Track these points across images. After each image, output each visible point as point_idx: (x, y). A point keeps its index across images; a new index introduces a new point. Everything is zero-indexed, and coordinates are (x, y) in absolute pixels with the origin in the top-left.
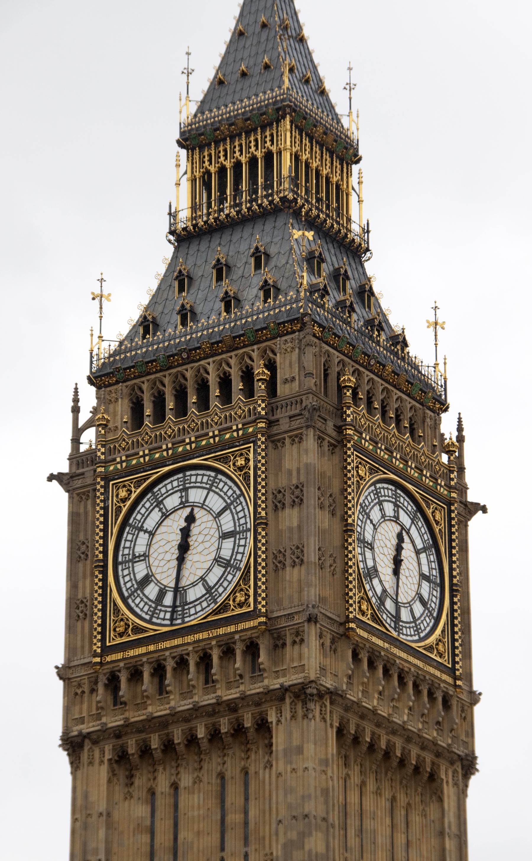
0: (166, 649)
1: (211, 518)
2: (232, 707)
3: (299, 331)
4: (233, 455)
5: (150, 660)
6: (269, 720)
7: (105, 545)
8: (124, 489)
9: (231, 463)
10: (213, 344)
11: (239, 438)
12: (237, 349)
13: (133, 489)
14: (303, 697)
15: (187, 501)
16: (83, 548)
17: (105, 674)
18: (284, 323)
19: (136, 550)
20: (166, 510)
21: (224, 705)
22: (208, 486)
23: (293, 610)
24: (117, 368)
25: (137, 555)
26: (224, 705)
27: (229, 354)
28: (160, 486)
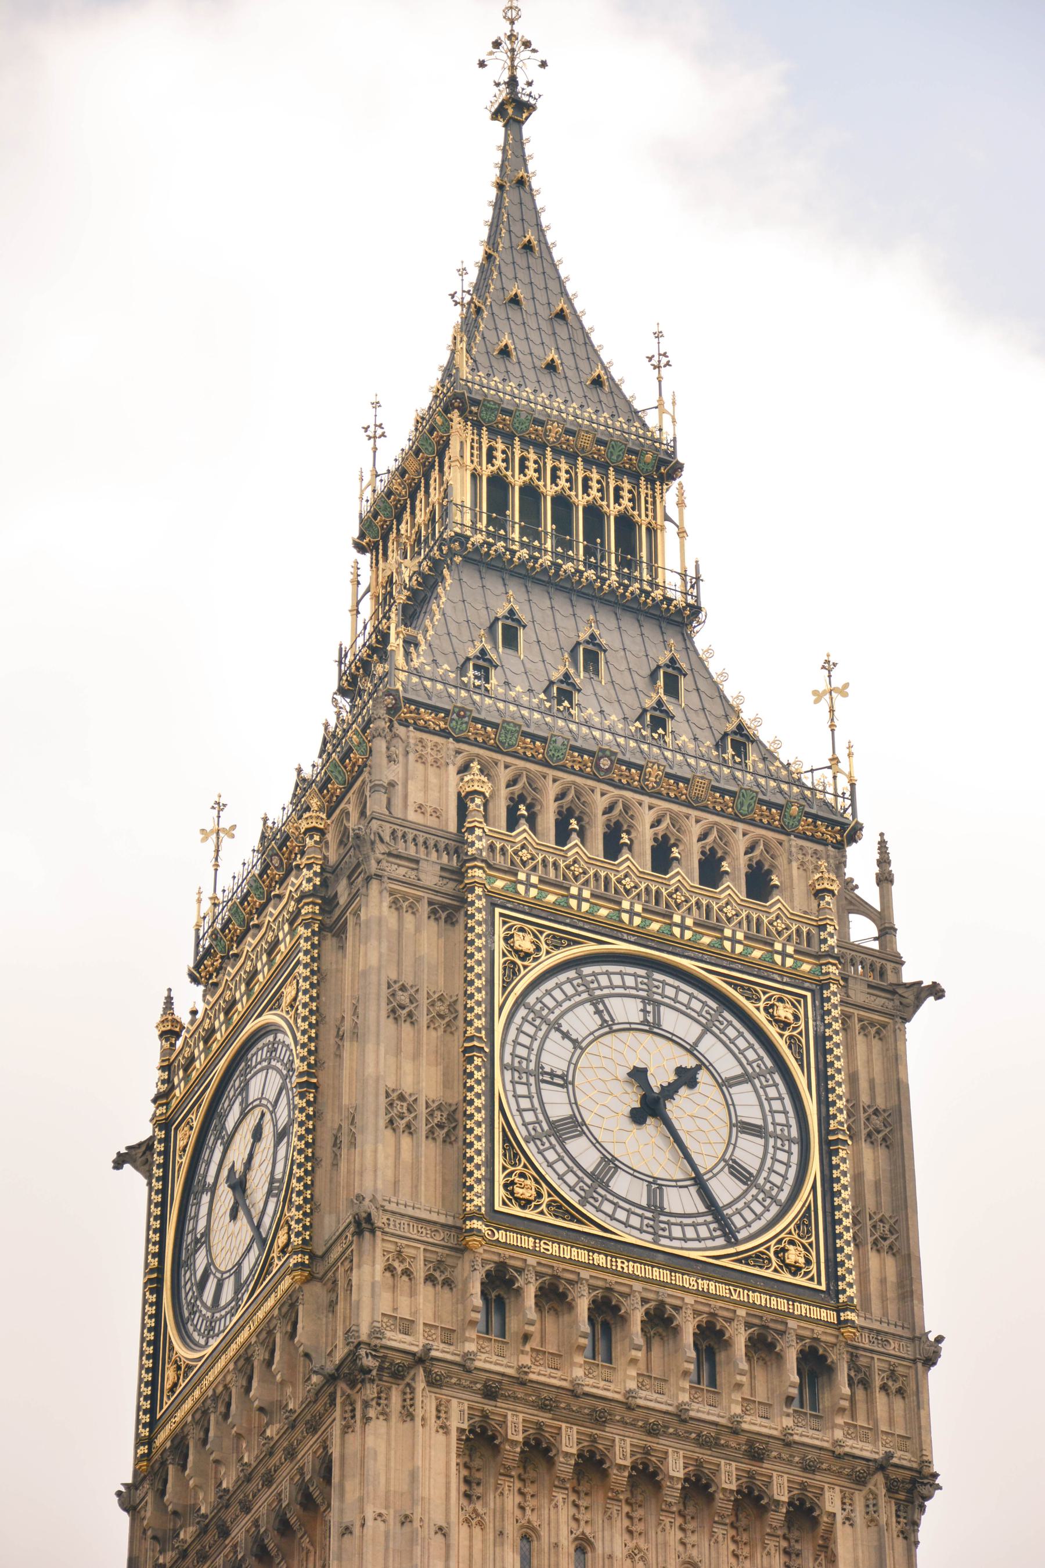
2: (755, 1450)
4: (765, 993)
10: (668, 776)
11: (782, 971)
12: (705, 809)
13: (544, 947)
14: (902, 1496)
17: (485, 1262)
18: (816, 817)
19: (542, 1059)
20: (612, 1020)
21: (742, 1439)
22: (704, 1021)
23: (884, 1327)
24: (462, 709)
25: (547, 1069)
26: (742, 1439)
27: (685, 810)
28: (597, 969)
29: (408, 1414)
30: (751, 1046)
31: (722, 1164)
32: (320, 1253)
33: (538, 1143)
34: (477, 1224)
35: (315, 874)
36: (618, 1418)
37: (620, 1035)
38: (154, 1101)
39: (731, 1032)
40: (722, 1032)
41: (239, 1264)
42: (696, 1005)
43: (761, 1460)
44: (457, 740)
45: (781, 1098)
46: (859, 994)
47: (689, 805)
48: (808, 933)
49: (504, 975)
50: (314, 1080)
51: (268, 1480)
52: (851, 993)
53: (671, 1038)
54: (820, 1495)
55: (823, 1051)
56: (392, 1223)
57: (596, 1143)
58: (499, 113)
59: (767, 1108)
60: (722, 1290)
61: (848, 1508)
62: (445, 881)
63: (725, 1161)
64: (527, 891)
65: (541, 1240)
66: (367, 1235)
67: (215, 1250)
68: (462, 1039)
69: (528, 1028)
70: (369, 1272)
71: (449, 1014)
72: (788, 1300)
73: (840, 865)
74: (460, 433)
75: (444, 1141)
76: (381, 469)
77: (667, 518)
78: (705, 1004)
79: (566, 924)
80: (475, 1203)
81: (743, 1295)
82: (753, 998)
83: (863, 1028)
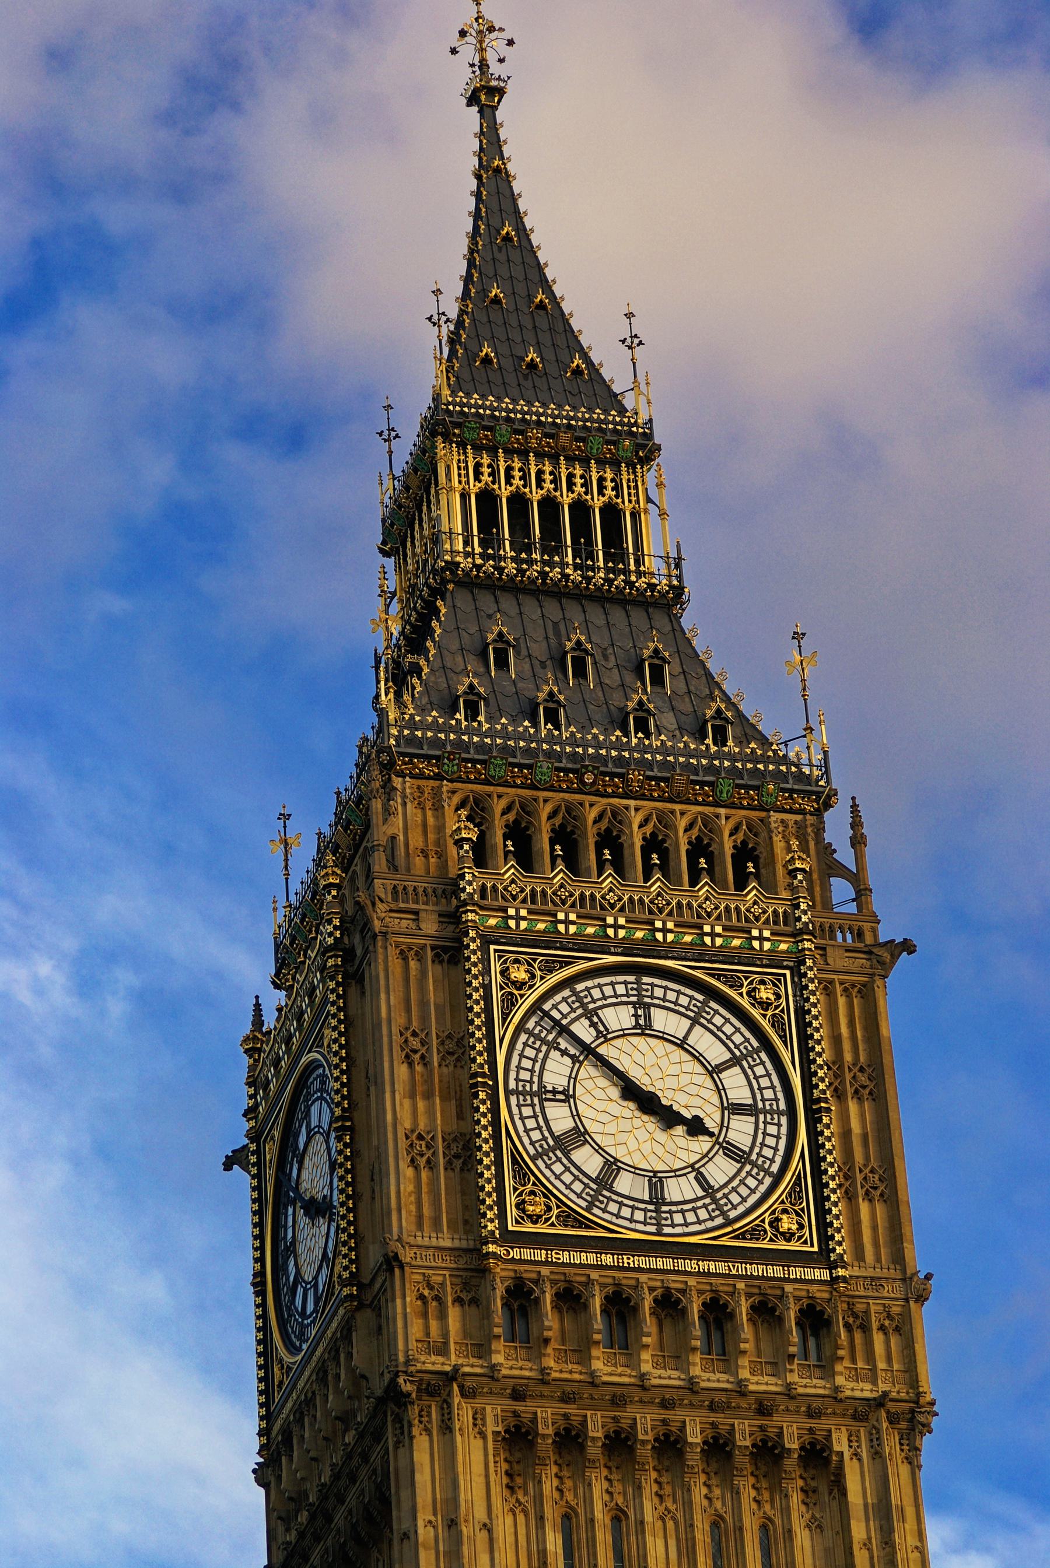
0: (640, 1270)
1: (699, 1069)
2: (764, 1408)
3: (811, 814)
5: (602, 1280)
6: (836, 1448)
8: (522, 968)
9: (744, 990)
12: (688, 802)
13: (538, 973)
15: (649, 1025)
16: (415, 1043)
18: (792, 791)
20: (606, 1029)
22: (692, 1014)
23: (878, 1273)
25: (549, 1088)
26: (752, 1399)
27: (669, 806)
28: (589, 983)
29: (447, 1428)
30: (737, 1030)
31: (717, 1147)
32: (366, 1281)
33: (545, 1158)
34: (492, 1248)
35: (336, 928)
36: (636, 1399)
37: (617, 1042)
38: (244, 1115)
39: (718, 1020)
40: (709, 1021)
41: (316, 1278)
42: (684, 1000)
43: (771, 1415)
44: (451, 781)
45: (768, 1075)
46: (838, 959)
47: (670, 800)
48: (785, 912)
49: (502, 1007)
50: (348, 1124)
51: (353, 1479)
52: (830, 960)
53: (663, 1037)
54: (829, 1437)
55: (803, 1026)
56: (418, 1256)
57: (599, 1149)
59: (756, 1086)
60: (722, 1267)
61: (855, 1444)
62: (445, 925)
63: (719, 1143)
64: (518, 925)
65: (552, 1250)
66: (397, 1271)
67: (301, 1261)
68: (467, 1076)
71: (457, 1048)
72: (783, 1266)
73: (820, 830)
75: (462, 1170)
76: (398, 473)
77: (649, 500)
78: (692, 998)
79: (556, 949)
80: (489, 1228)
81: (740, 1268)
82: (736, 985)
83: (846, 990)
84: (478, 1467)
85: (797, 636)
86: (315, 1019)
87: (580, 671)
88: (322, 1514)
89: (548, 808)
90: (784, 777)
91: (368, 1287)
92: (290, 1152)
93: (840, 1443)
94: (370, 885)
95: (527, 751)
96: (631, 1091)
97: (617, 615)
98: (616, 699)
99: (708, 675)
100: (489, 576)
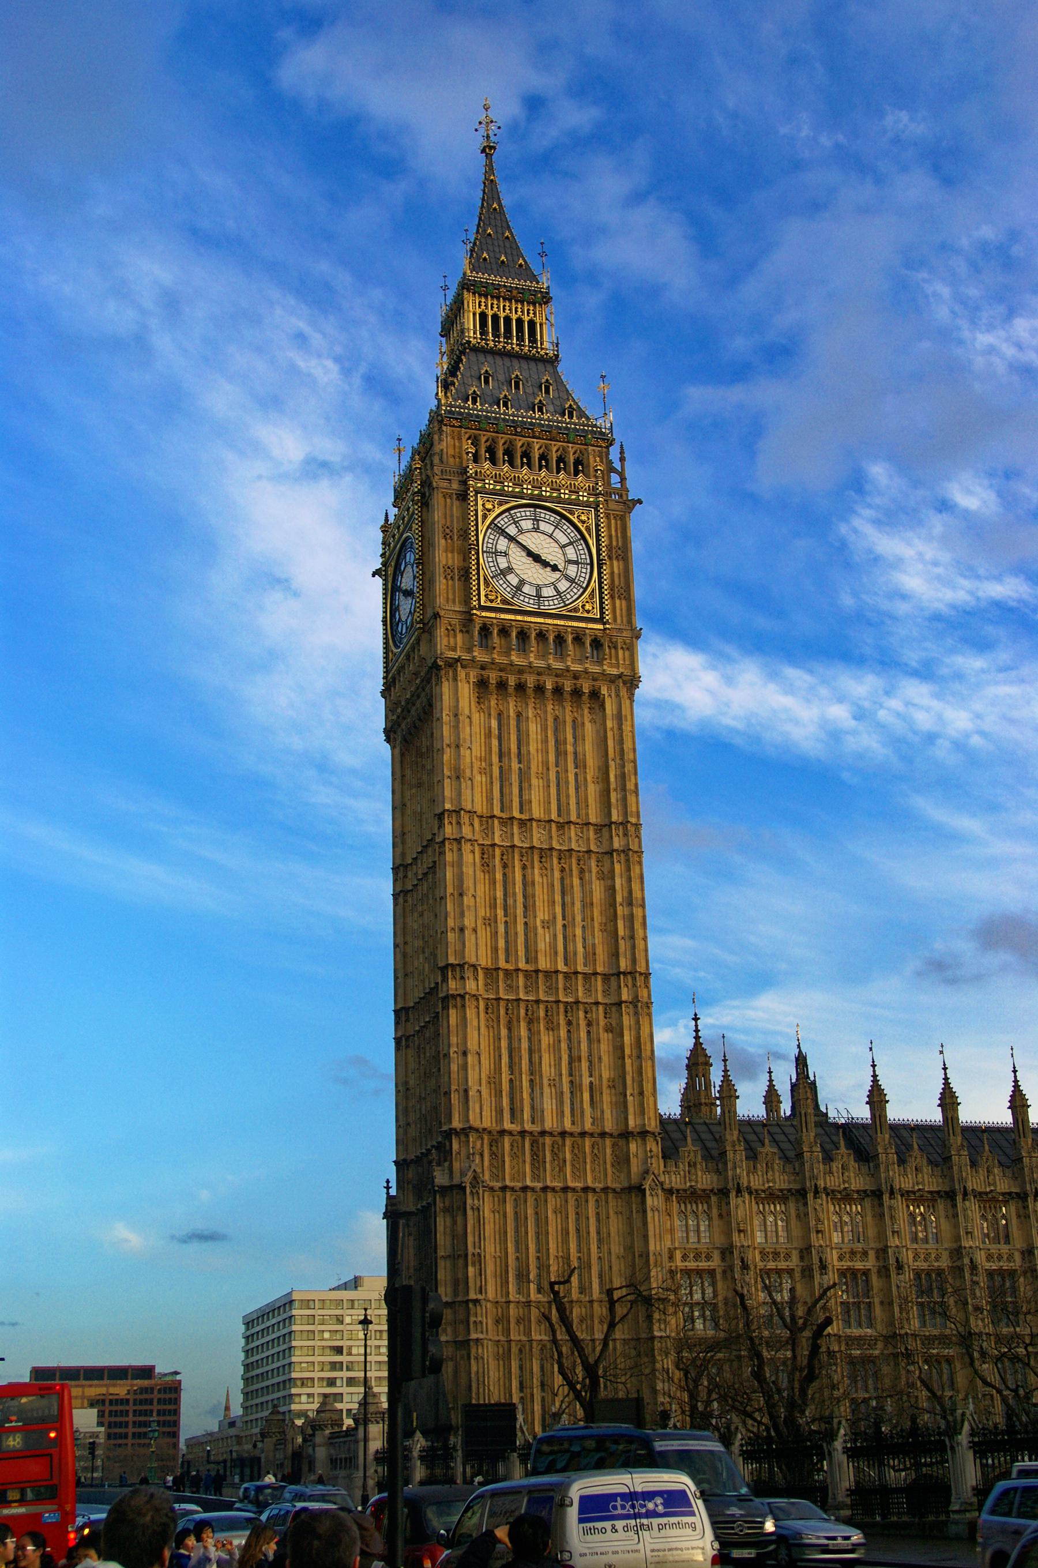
2: (576, 676)
7: (477, 535)
16: (448, 531)
29: (455, 679)
42: (552, 519)
46: (612, 505)
51: (419, 697)
55: (598, 531)
57: (517, 575)
58: (483, 151)
60: (562, 623)
69: (492, 537)
70: (440, 632)
71: (464, 534)
73: (608, 454)
74: (469, 299)
81: (570, 623)
82: (572, 513)
84: (467, 695)
85: (603, 377)
86: (409, 521)
87: (517, 387)
88: (406, 710)
89: (503, 441)
90: (595, 433)
91: (427, 625)
92: (398, 571)
93: (604, 691)
94: (432, 469)
95: (495, 418)
96: (530, 554)
97: (532, 365)
98: (531, 399)
99: (567, 391)
100: (483, 347)
